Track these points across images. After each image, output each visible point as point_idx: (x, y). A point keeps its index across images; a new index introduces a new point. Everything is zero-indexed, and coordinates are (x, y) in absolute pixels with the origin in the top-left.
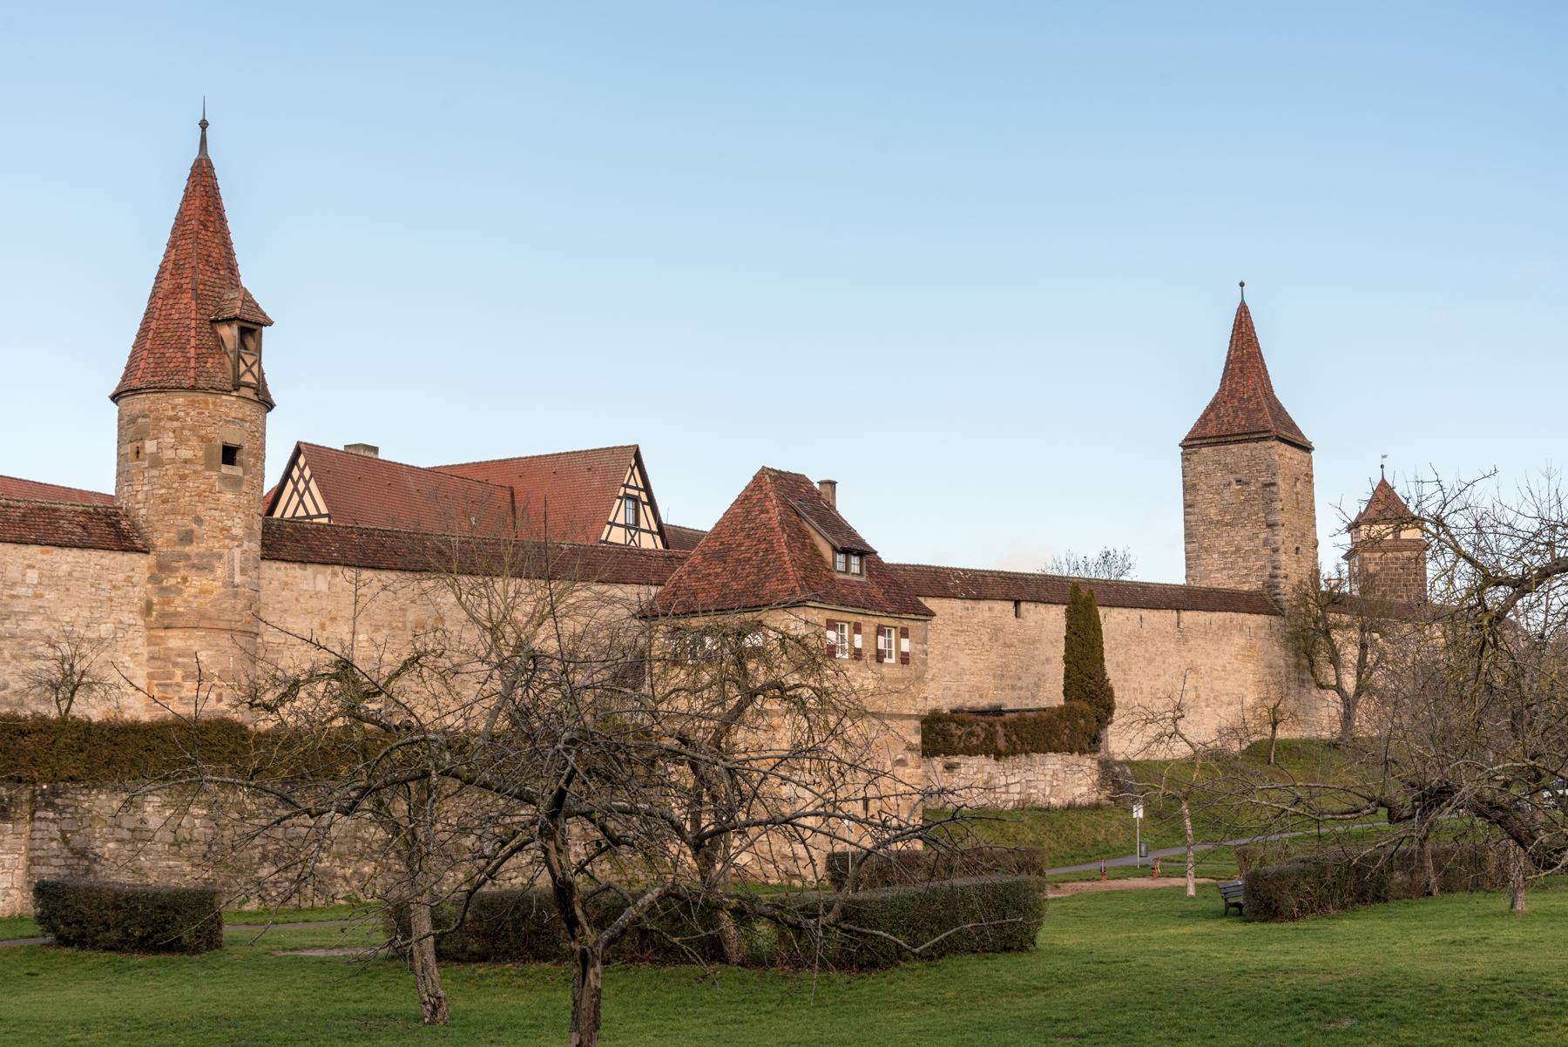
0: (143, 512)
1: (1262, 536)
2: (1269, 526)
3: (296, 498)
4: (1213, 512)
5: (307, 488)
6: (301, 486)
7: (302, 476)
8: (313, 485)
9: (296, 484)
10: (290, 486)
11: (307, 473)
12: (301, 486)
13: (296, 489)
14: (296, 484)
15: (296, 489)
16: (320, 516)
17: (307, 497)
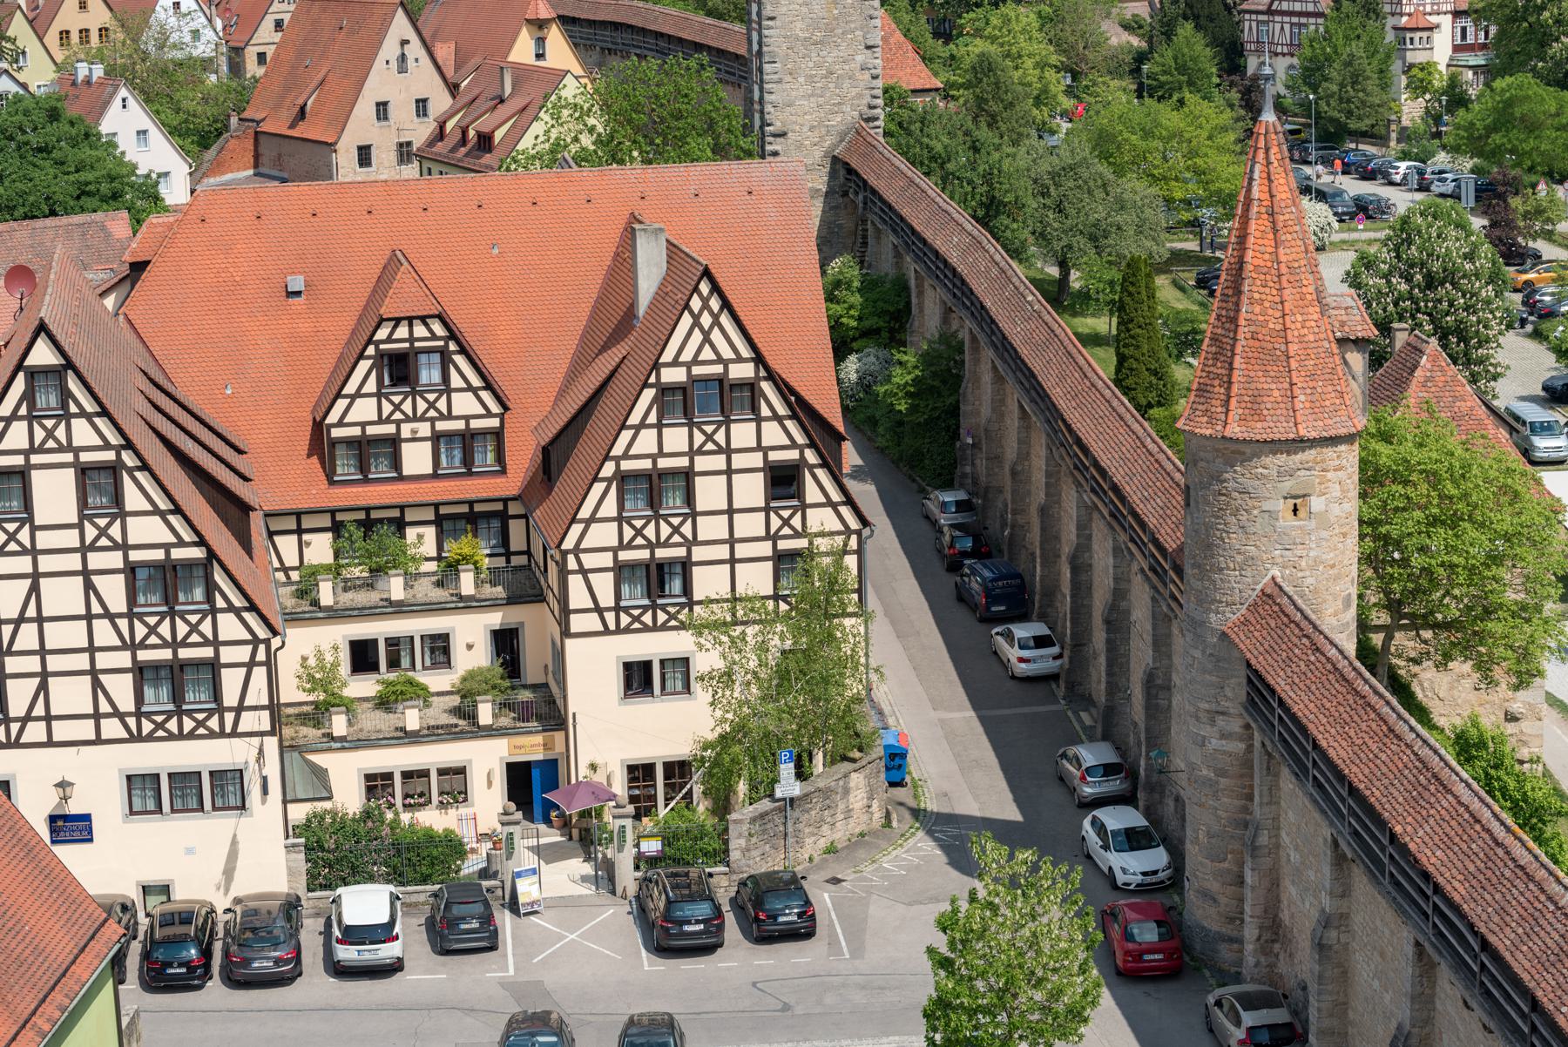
0: (1309, 581)
1: (859, 58)
2: (868, 47)
3: (697, 337)
4: (799, 28)
5: (716, 322)
6: (706, 320)
7: (706, 306)
8: (725, 320)
9: (696, 318)
10: (687, 320)
11: (715, 304)
12: (706, 320)
13: (696, 323)
14: (696, 318)
15: (696, 323)
16: (739, 359)
17: (716, 336)
